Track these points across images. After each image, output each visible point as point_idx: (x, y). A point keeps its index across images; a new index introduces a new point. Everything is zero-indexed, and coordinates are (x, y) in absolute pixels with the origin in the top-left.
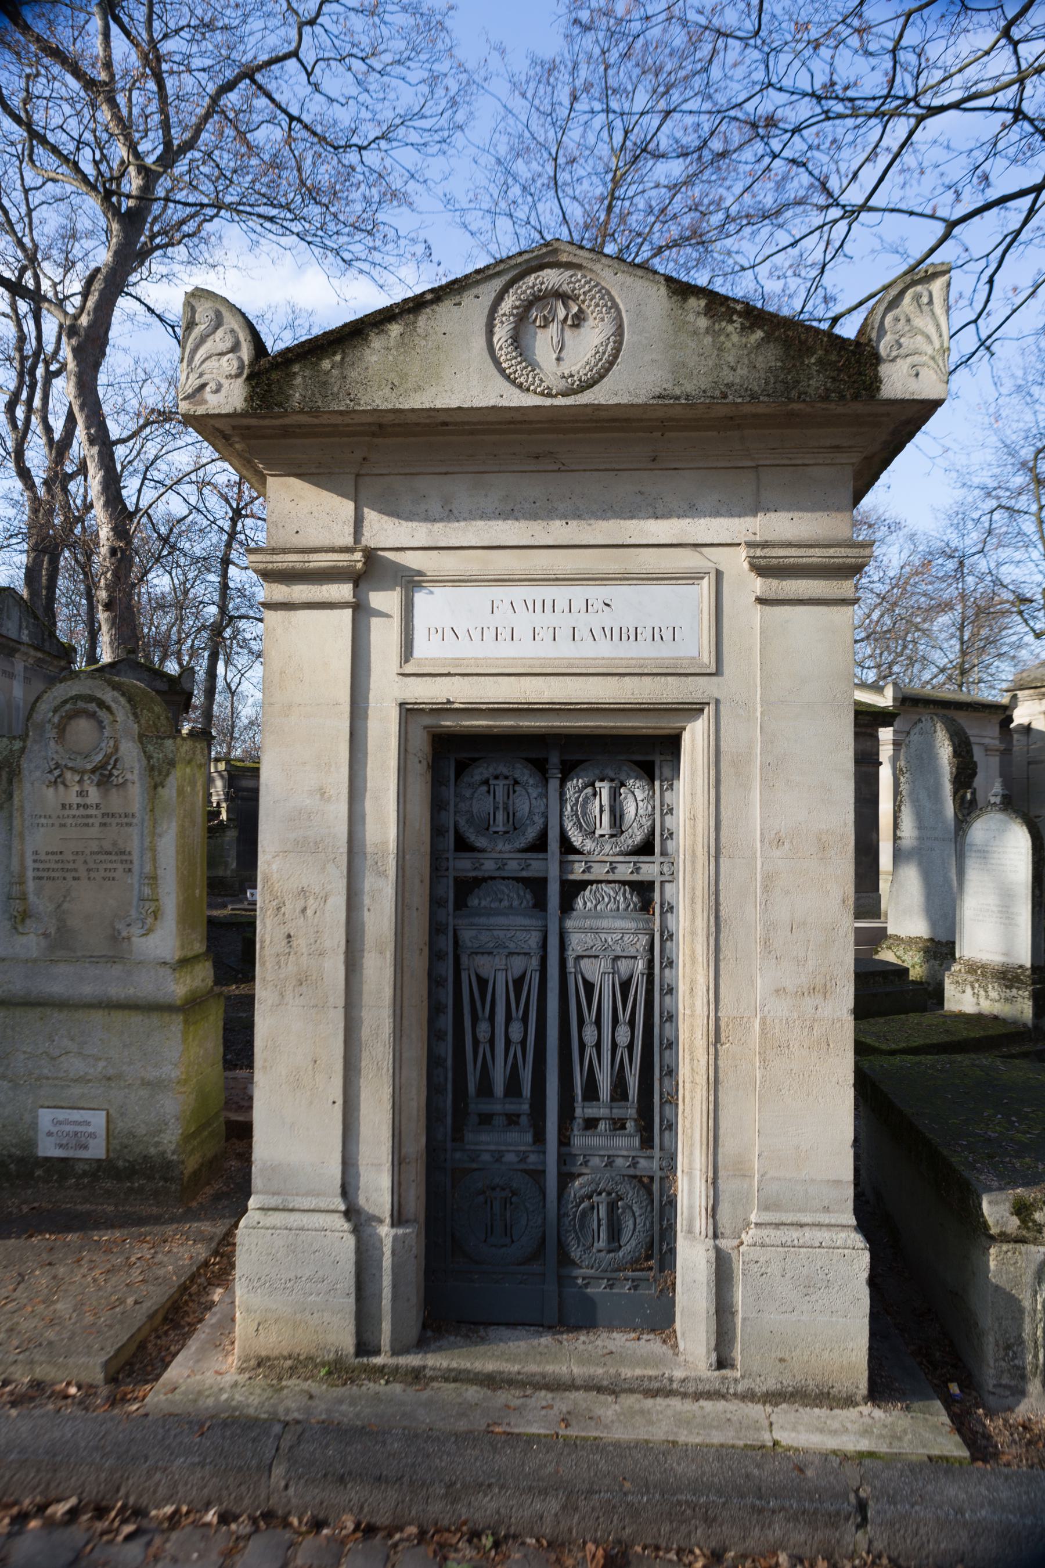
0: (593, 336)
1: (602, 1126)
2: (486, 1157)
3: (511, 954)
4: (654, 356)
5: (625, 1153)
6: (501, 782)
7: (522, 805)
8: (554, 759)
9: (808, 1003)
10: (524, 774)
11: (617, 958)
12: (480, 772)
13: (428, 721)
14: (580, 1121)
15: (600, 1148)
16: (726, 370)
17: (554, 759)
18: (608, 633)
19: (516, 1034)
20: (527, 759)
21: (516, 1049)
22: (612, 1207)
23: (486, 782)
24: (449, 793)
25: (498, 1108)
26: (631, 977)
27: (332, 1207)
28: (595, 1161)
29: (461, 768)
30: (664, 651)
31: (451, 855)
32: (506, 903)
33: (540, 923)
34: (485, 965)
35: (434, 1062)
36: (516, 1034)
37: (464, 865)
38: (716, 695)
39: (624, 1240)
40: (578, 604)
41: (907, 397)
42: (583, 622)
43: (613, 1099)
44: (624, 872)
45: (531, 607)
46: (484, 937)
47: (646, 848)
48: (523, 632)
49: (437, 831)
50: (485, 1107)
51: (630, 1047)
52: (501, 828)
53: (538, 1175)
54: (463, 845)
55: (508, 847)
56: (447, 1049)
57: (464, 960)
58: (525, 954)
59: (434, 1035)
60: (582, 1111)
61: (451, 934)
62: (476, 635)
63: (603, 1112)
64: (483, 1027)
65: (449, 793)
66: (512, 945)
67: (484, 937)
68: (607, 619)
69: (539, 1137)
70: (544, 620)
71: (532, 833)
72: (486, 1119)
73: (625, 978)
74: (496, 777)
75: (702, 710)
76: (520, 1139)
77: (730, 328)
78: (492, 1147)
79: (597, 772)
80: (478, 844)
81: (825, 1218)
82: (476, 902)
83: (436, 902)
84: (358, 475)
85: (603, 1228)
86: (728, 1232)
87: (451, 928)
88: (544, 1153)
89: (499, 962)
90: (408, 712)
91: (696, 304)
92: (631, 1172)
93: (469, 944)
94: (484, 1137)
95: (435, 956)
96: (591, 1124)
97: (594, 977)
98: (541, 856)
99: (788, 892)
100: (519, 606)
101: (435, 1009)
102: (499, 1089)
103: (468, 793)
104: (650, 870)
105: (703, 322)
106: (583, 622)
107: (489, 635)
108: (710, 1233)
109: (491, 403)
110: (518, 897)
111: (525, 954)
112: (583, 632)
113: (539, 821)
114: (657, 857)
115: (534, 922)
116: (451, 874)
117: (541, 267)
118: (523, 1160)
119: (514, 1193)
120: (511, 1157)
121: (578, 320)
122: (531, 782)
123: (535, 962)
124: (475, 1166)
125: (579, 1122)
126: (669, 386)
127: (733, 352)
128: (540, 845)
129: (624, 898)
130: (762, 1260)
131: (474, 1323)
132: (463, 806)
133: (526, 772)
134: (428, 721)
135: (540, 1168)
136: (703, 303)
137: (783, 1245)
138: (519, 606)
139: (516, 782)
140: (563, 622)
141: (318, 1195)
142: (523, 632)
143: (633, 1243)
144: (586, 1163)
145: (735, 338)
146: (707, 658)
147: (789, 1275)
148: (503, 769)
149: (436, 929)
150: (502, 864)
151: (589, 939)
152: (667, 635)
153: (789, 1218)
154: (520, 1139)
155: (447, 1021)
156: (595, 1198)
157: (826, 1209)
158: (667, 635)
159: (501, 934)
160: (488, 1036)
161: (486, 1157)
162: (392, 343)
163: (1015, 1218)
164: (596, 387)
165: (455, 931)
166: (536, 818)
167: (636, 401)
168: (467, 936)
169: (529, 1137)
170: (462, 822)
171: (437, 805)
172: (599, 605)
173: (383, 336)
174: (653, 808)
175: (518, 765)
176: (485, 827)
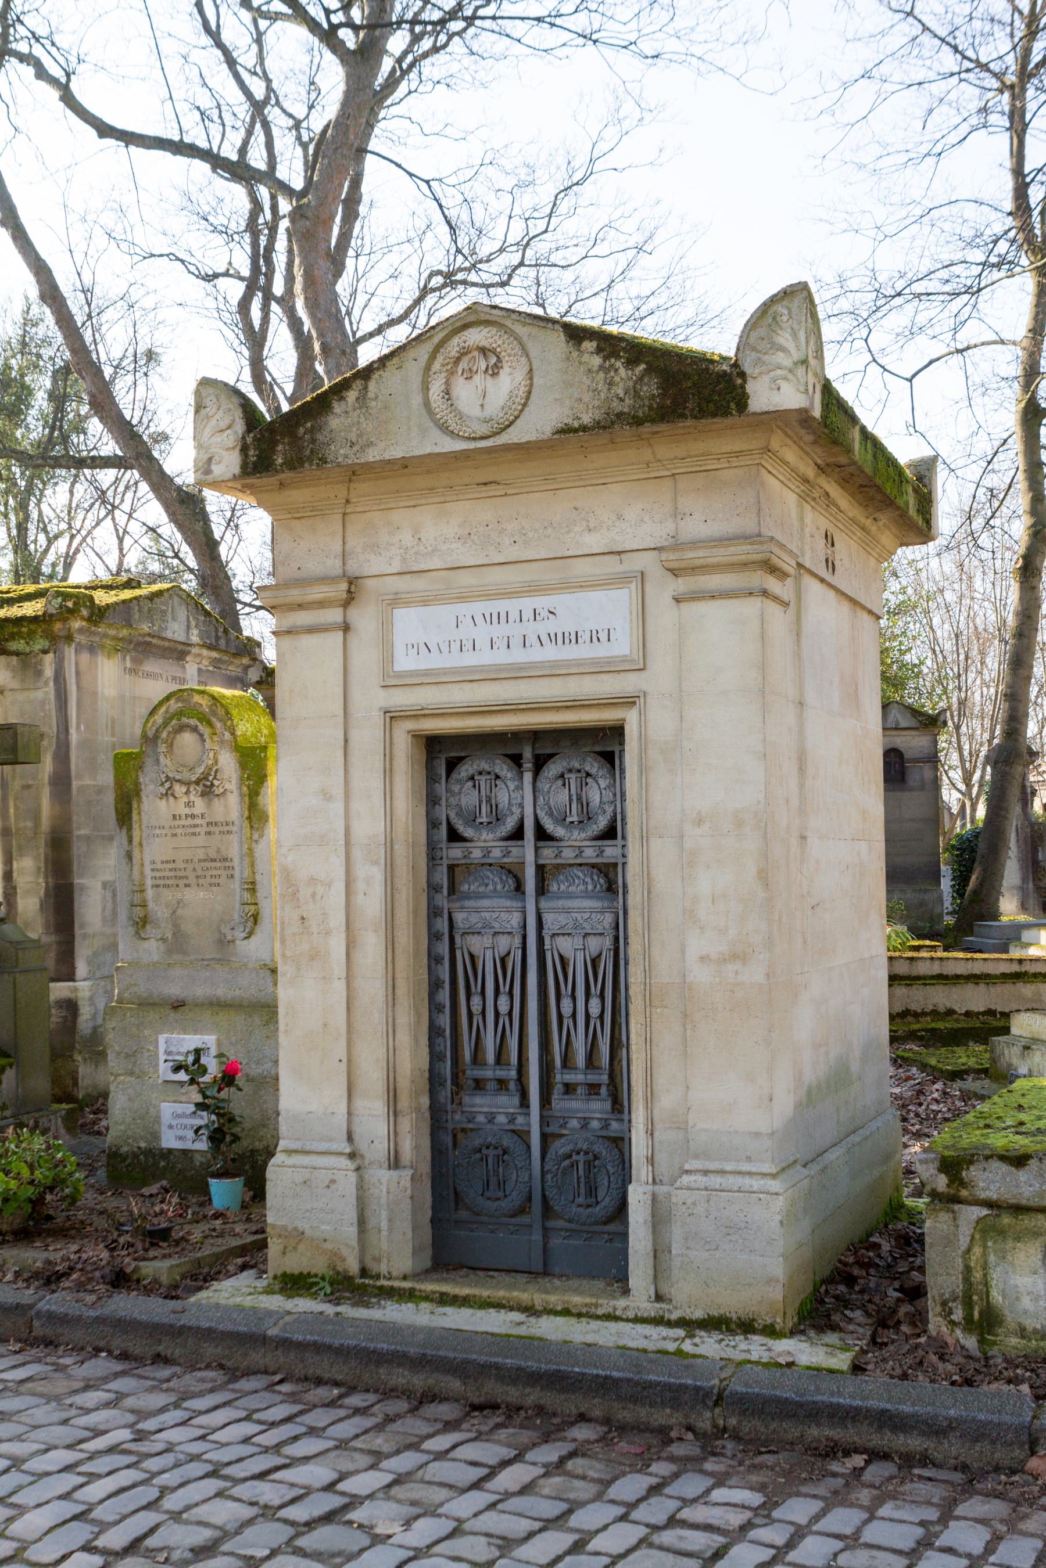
0: (506, 384)
1: (579, 1090)
2: (481, 1118)
3: (495, 934)
4: (557, 396)
5: (598, 1116)
6: (483, 778)
7: (502, 796)
8: (528, 754)
9: (730, 968)
10: (503, 769)
11: (586, 935)
12: (465, 770)
13: (411, 725)
14: (560, 1086)
15: (577, 1111)
16: (615, 403)
17: (528, 754)
18: (553, 638)
19: (503, 1008)
20: (506, 755)
21: (504, 1019)
22: (589, 1165)
23: (472, 778)
24: (441, 788)
25: (489, 1074)
26: (600, 955)
27: (339, 1150)
28: (574, 1123)
29: (452, 765)
30: (601, 651)
31: (444, 845)
32: (491, 887)
33: (520, 904)
34: (477, 944)
35: (434, 1032)
36: (503, 1008)
37: (456, 852)
38: (644, 688)
39: (601, 1194)
40: (528, 614)
41: (772, 409)
42: (532, 629)
43: (587, 1067)
44: (590, 854)
45: (488, 618)
46: (474, 918)
47: (610, 833)
48: (483, 643)
49: (432, 824)
50: (478, 1073)
51: (601, 1016)
52: (484, 819)
53: (523, 1136)
54: (454, 836)
55: (491, 836)
56: (445, 1020)
57: (458, 939)
58: (509, 933)
59: (435, 1008)
60: (560, 1077)
61: (446, 916)
62: (445, 648)
63: (580, 1078)
64: (476, 1000)
65: (441, 788)
66: (497, 925)
67: (474, 918)
68: (552, 626)
69: (525, 1103)
70: (498, 631)
71: (510, 824)
72: (479, 1085)
73: (595, 954)
74: (480, 773)
75: (634, 703)
76: (508, 1102)
77: (618, 364)
78: (486, 1110)
79: (565, 764)
80: (466, 835)
81: (746, 1167)
82: (466, 887)
83: (433, 888)
84: (344, 514)
85: (582, 1185)
86: (666, 1180)
87: (446, 911)
88: (529, 1114)
89: (487, 941)
90: (393, 717)
91: (589, 345)
92: (604, 1133)
93: (461, 925)
94: (478, 1100)
95: (434, 936)
96: (569, 1089)
97: (568, 953)
98: (519, 843)
99: (708, 867)
100: (479, 619)
101: (435, 985)
102: (491, 1057)
103: (456, 788)
104: (611, 851)
105: (597, 361)
106: (532, 629)
107: (455, 647)
108: (650, 1180)
109: (428, 451)
110: (496, 881)
111: (509, 933)
112: (532, 639)
113: (517, 811)
114: (619, 841)
115: (515, 904)
116: (445, 862)
117: (466, 326)
118: (512, 1121)
119: (505, 1152)
120: (501, 1119)
121: (494, 371)
122: (509, 775)
123: (517, 941)
124: (471, 1126)
125: (558, 1089)
126: (570, 421)
127: (621, 385)
128: (518, 834)
129: (592, 882)
130: (689, 1202)
131: (473, 1269)
132: (453, 801)
133: (596, 765)
134: (411, 725)
135: (526, 1128)
136: (594, 344)
137: (706, 1189)
138: (479, 619)
139: (497, 777)
140: (516, 631)
141: (331, 1140)
142: (483, 643)
143: (607, 1199)
144: (564, 1126)
145: (622, 372)
146: (637, 655)
147: (712, 1217)
148: (485, 766)
149: (434, 912)
150: (487, 852)
151: (562, 919)
152: (603, 636)
153: (712, 1166)
154: (508, 1102)
155: (444, 996)
156: (575, 1157)
157: (749, 1159)
158: (603, 636)
159: (487, 915)
160: (480, 1008)
161: (481, 1118)
162: (350, 409)
163: (943, 1176)
164: (509, 430)
165: (450, 913)
166: (514, 809)
167: (542, 437)
168: (459, 917)
169: (516, 1100)
170: (452, 815)
171: (432, 801)
172: (545, 613)
173: (343, 403)
174: (615, 795)
175: (498, 761)
176: (472, 820)
